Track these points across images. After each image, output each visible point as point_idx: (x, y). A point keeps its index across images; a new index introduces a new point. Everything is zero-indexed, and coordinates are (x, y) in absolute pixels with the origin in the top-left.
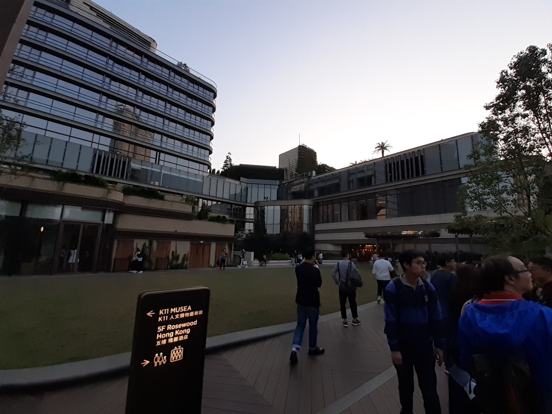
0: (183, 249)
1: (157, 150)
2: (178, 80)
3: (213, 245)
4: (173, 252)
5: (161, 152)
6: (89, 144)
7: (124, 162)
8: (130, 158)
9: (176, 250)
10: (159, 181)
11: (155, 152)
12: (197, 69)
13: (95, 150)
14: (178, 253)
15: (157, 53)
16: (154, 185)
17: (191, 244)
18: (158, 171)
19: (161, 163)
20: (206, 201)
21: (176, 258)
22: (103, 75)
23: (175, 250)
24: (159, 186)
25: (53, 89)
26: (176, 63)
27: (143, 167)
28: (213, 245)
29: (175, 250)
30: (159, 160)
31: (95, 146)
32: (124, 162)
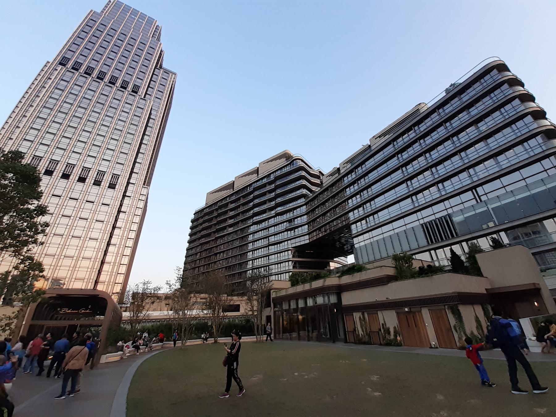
0: (390, 319)
1: (470, 189)
2: (466, 97)
3: (426, 313)
4: (383, 324)
5: (475, 187)
6: (417, 223)
7: (447, 221)
8: (449, 215)
9: (385, 322)
10: (491, 220)
11: (470, 192)
12: (461, 74)
13: (422, 225)
14: (387, 326)
15: (429, 105)
16: (488, 228)
17: (398, 313)
18: (485, 209)
19: (484, 198)
20: (494, 236)
21: (388, 331)
22: (449, 139)
23: (383, 322)
24: (496, 226)
25: (385, 202)
26: (444, 94)
27: (466, 215)
28: (426, 313)
29: (383, 322)
30: (479, 197)
31: (422, 222)
32: (447, 221)
